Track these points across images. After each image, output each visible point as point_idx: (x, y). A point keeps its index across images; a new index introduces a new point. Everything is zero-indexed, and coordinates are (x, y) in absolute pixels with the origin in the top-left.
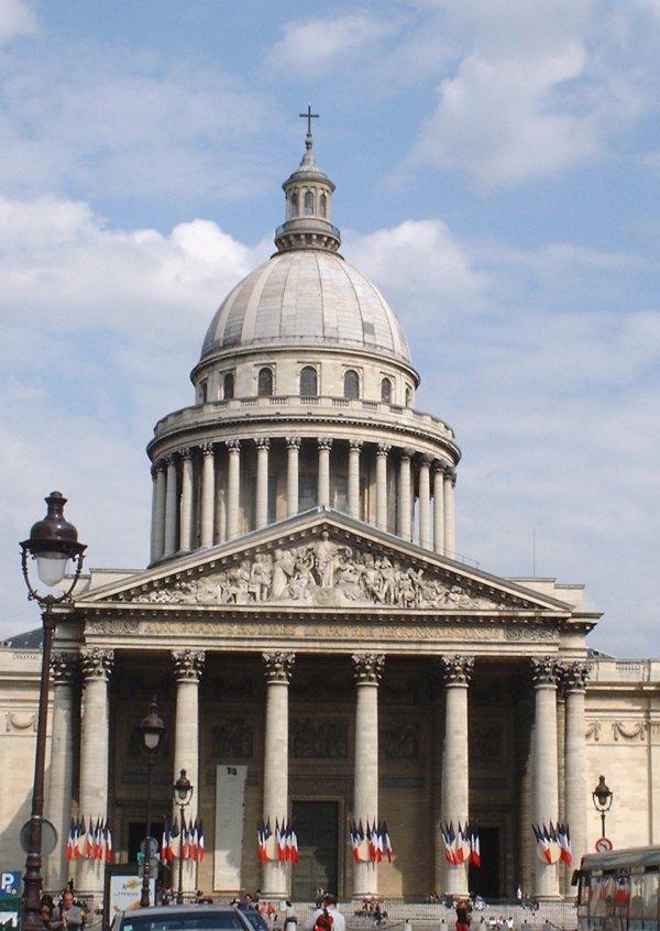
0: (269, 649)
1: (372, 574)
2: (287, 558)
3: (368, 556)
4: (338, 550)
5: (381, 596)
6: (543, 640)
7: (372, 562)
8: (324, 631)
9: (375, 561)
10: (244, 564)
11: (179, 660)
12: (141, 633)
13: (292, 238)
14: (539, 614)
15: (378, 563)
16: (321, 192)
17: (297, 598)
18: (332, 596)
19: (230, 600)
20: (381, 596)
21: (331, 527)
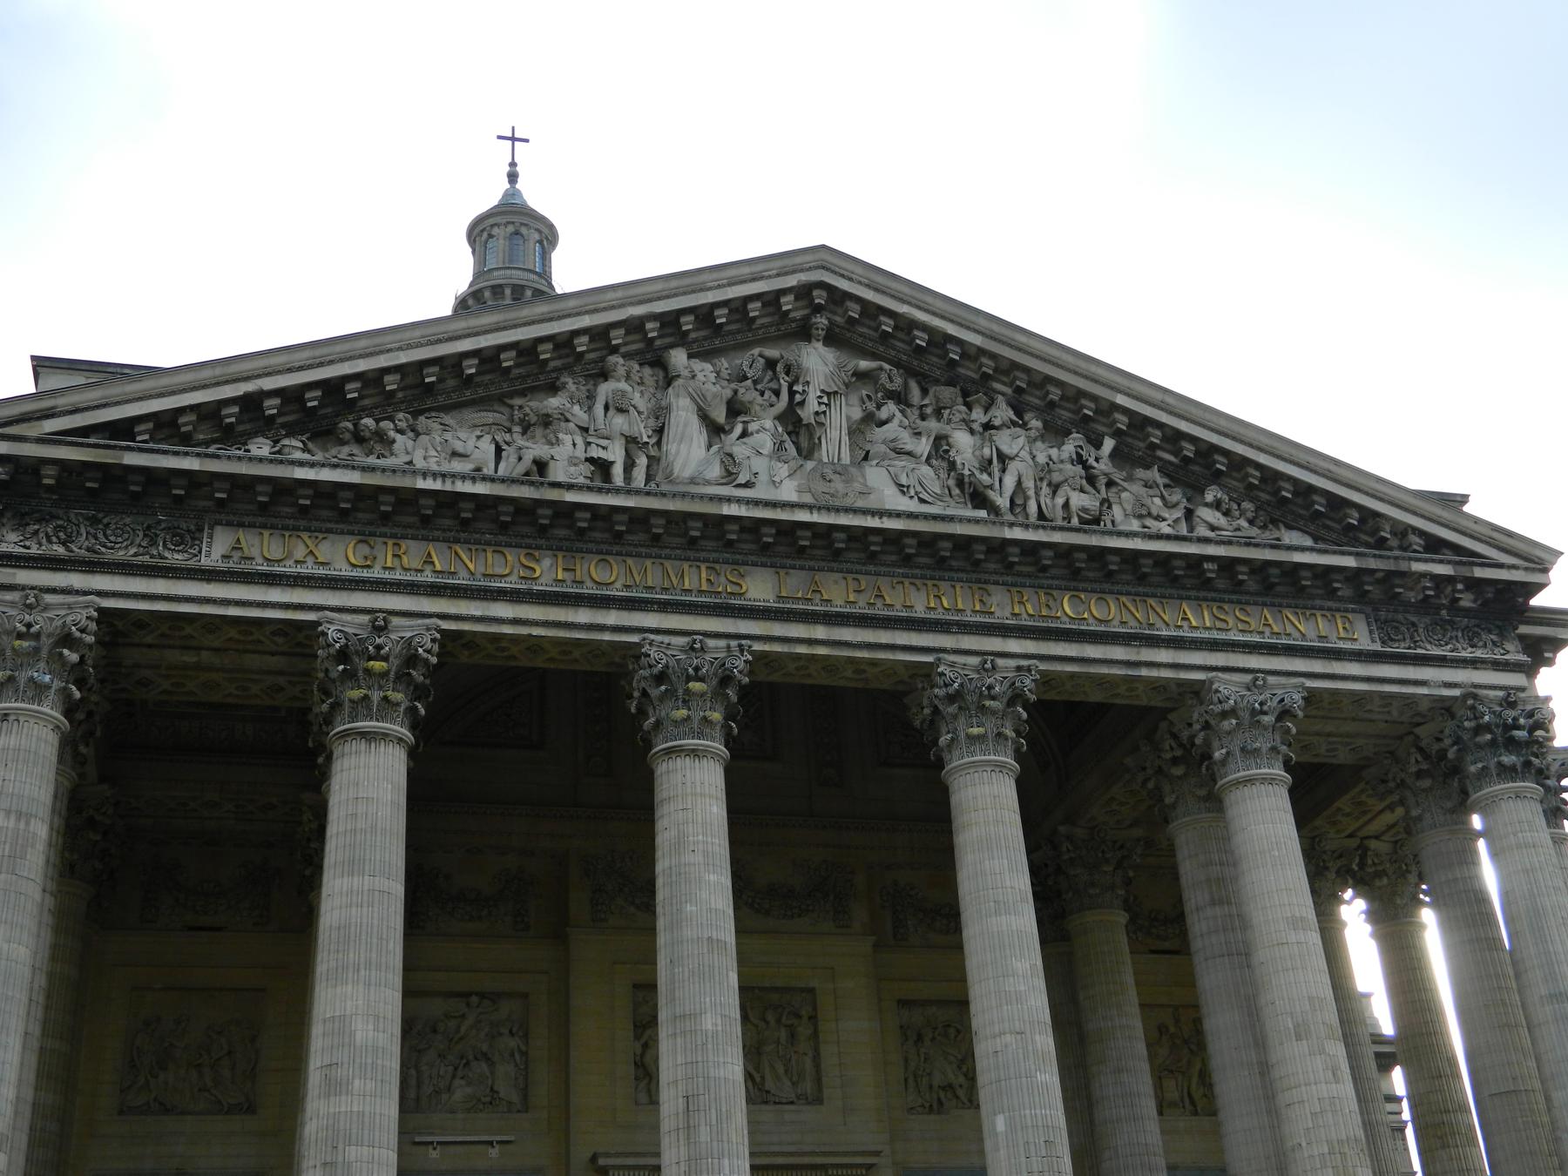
0: (662, 633)
1: (963, 441)
2: (702, 377)
3: (947, 393)
4: (861, 376)
5: (1003, 502)
6: (1479, 653)
7: (964, 408)
8: (837, 592)
9: (969, 407)
10: (570, 381)
11: (343, 655)
12: (205, 561)
13: (487, 294)
14: (1465, 571)
15: (978, 415)
16: (537, 236)
17: (748, 485)
18: (857, 486)
19: (527, 474)
20: (1003, 502)
21: (838, 298)
